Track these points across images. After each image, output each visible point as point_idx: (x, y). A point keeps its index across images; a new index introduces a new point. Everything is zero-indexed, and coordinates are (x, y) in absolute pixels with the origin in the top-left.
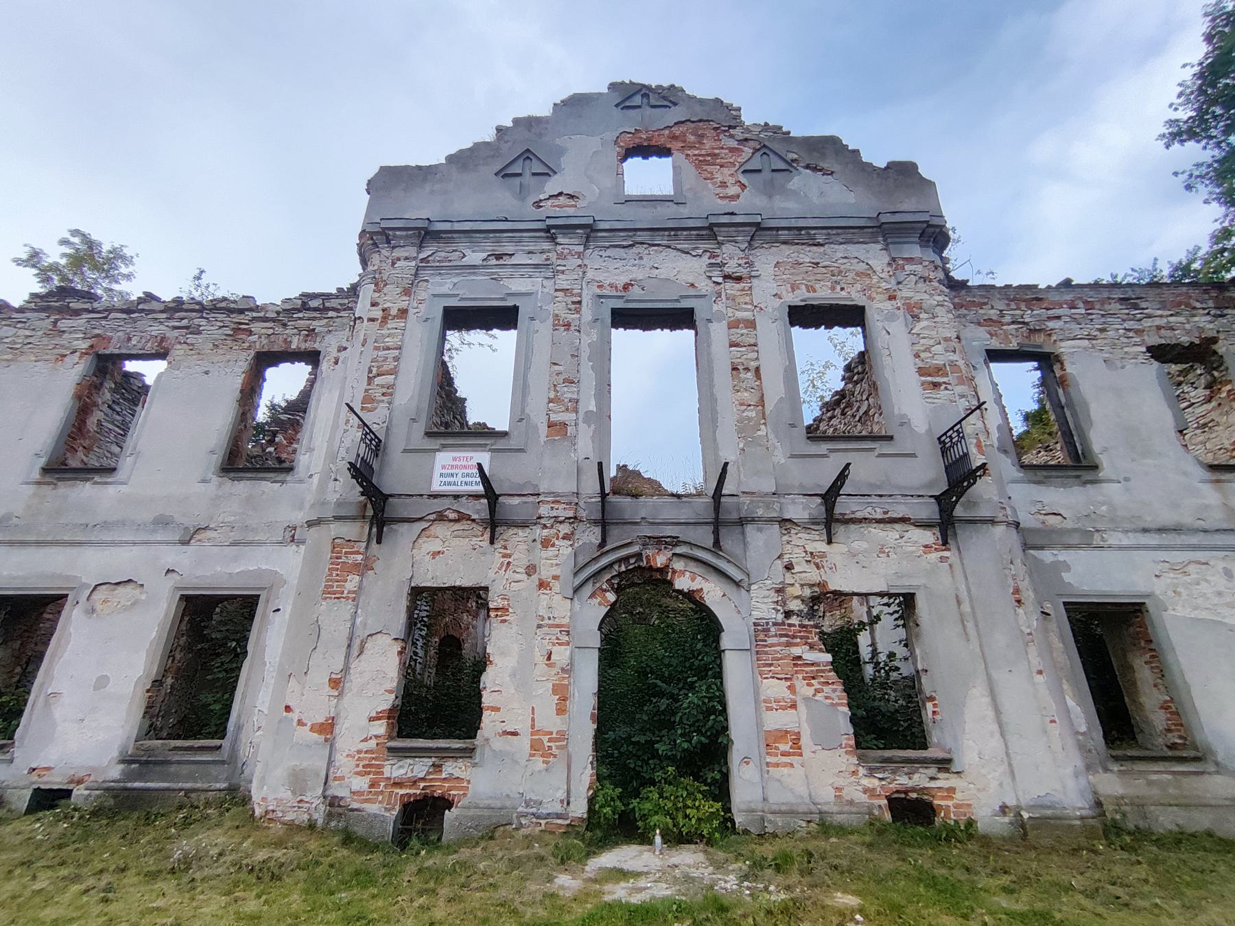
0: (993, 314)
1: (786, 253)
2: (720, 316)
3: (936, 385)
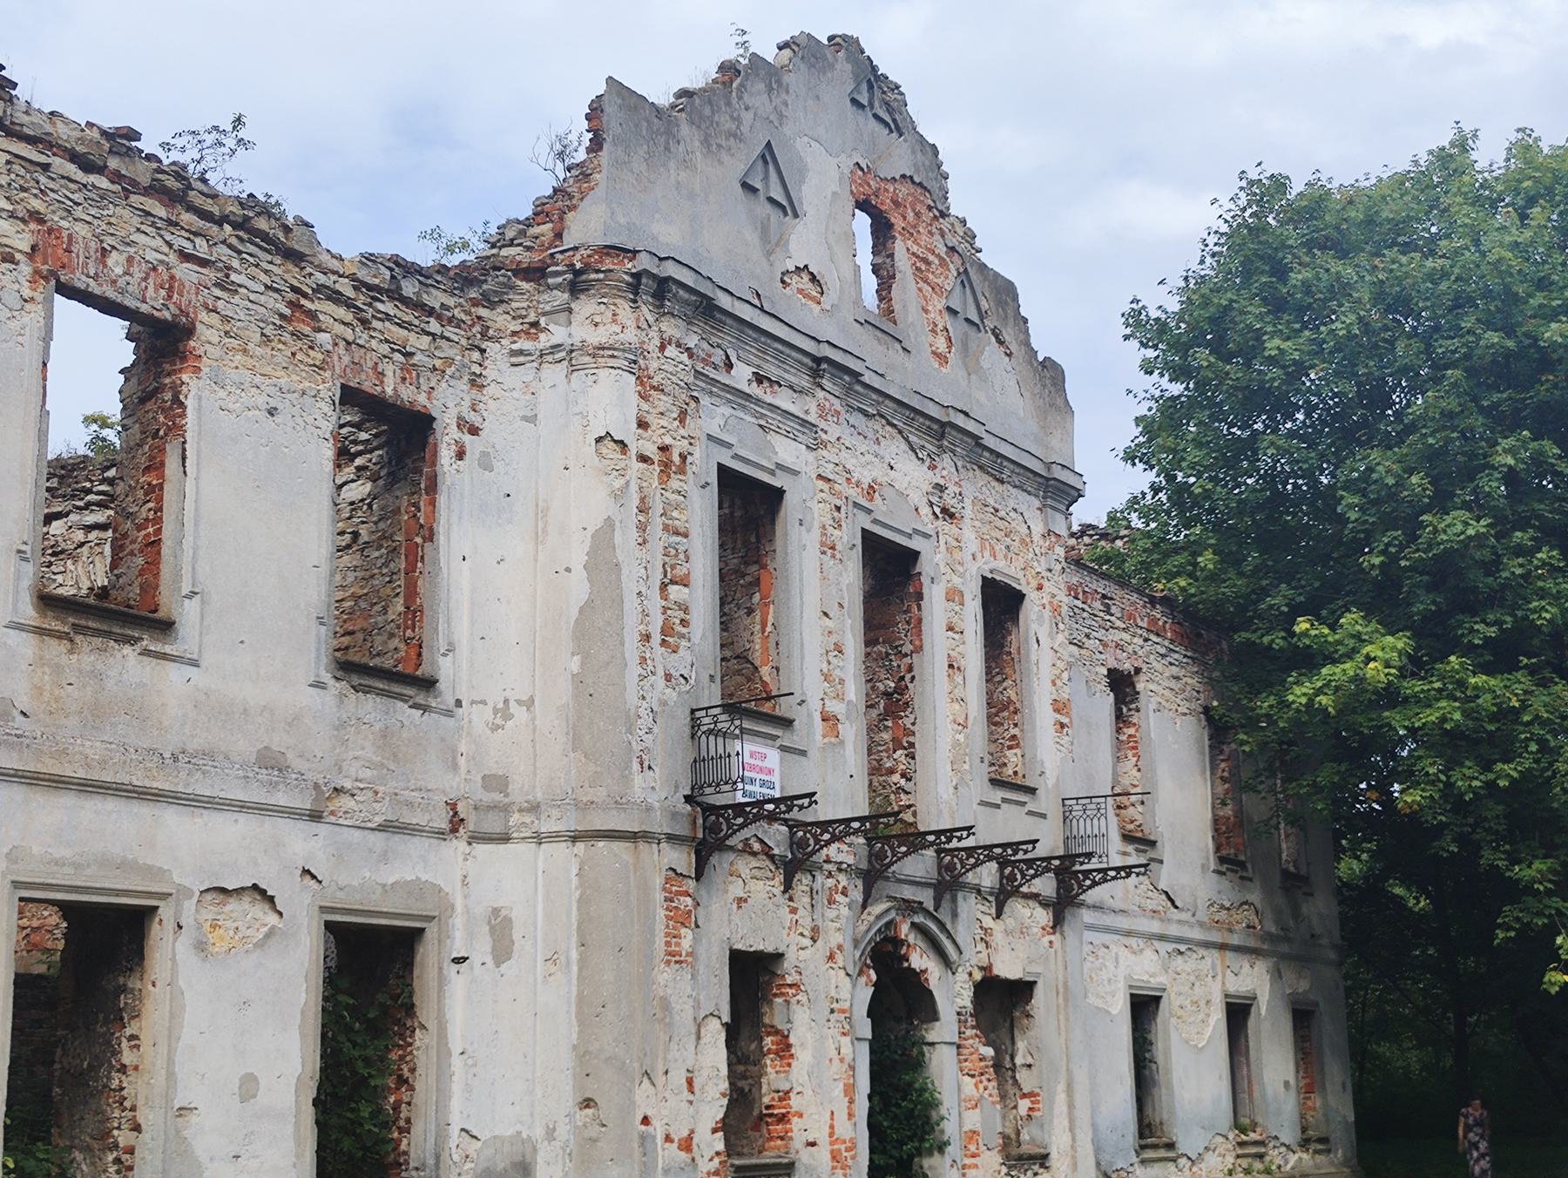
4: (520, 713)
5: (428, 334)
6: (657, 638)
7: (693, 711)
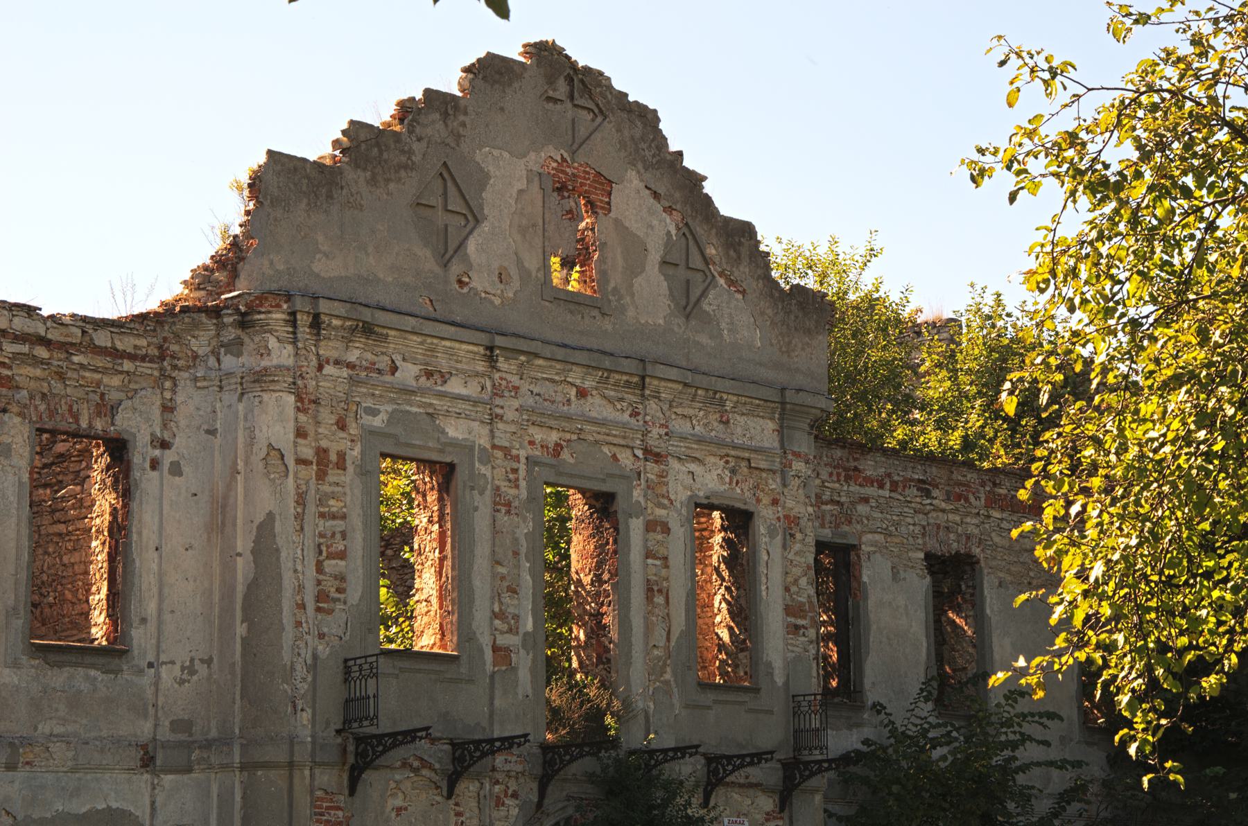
2: (641, 511)
3: (797, 627)
4: (202, 670)
5: (121, 372)
6: (310, 606)
7: (346, 661)
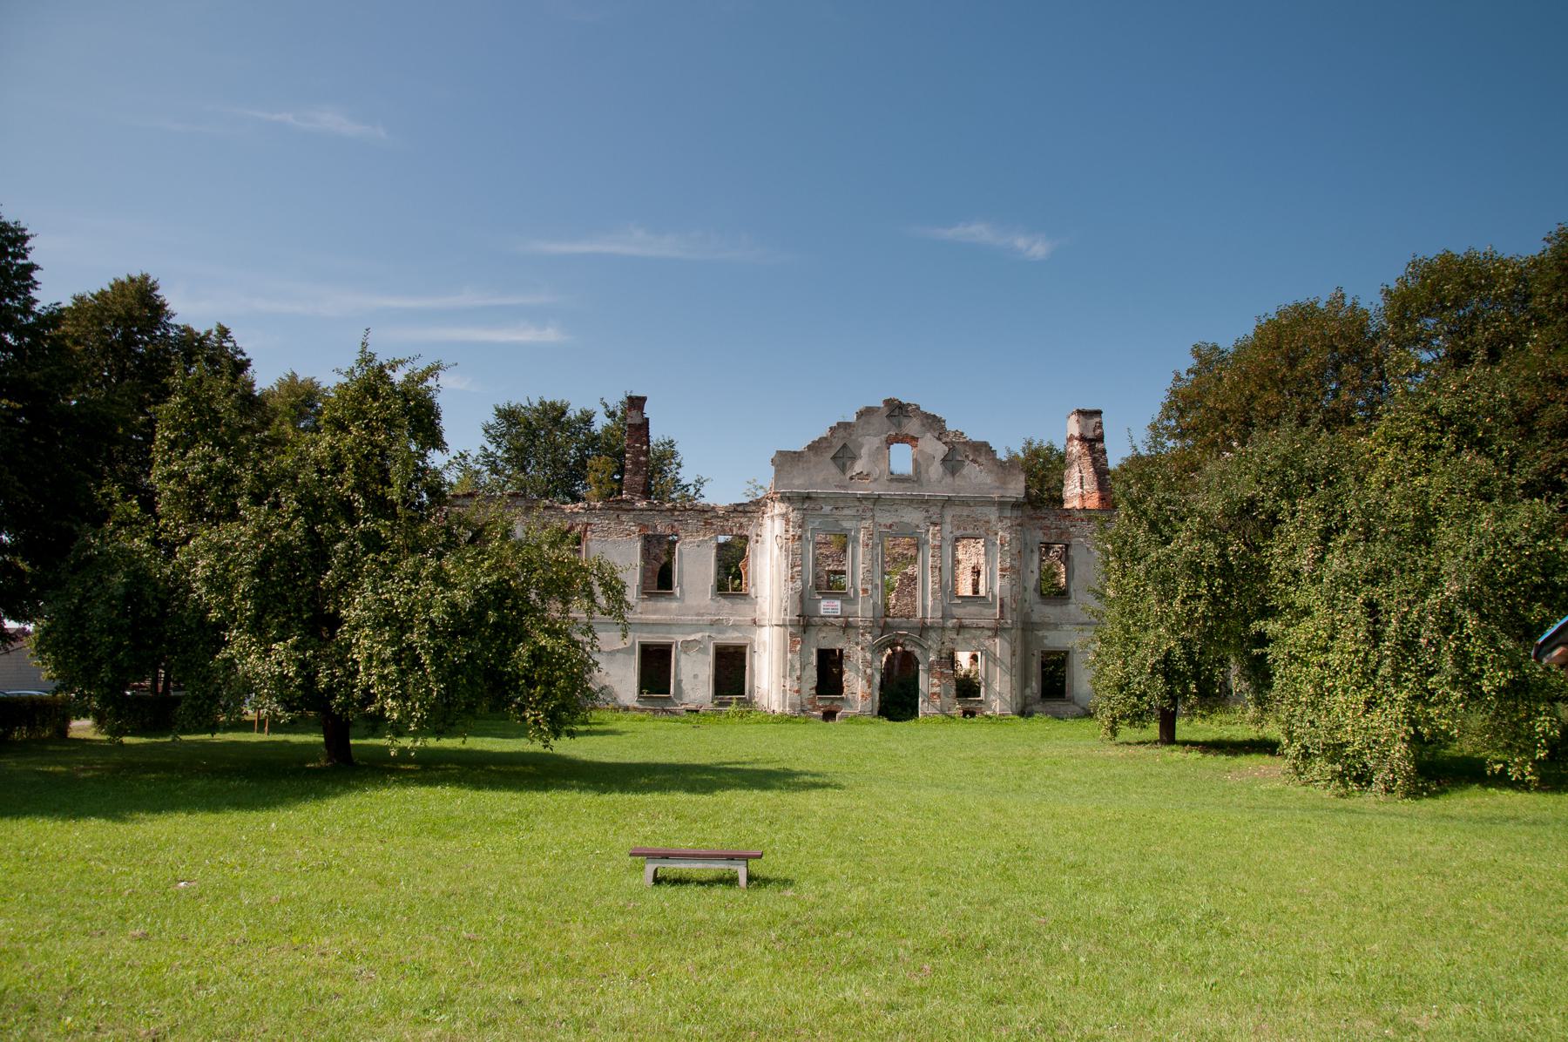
0: (1047, 523)
1: (958, 510)
